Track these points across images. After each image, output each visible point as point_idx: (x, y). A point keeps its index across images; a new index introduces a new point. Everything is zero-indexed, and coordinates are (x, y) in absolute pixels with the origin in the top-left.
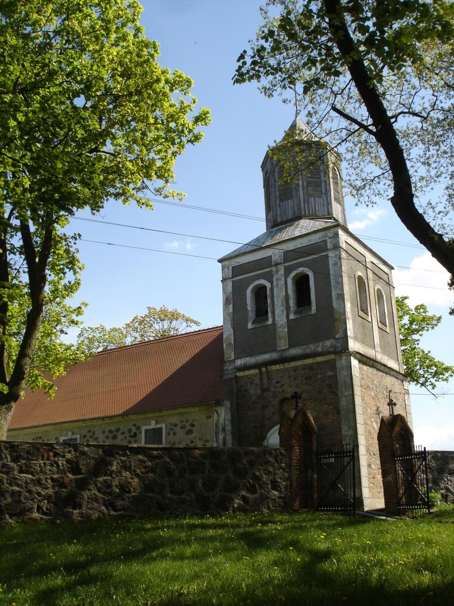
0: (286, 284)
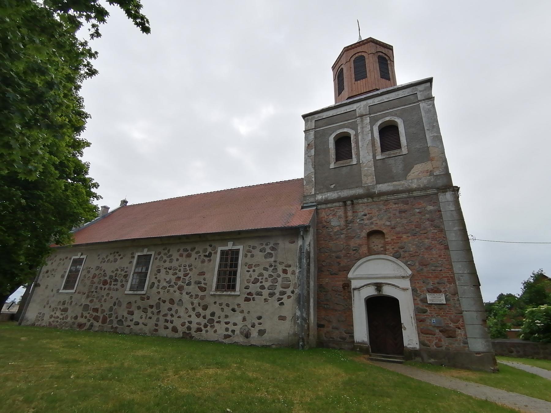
0: (372, 130)
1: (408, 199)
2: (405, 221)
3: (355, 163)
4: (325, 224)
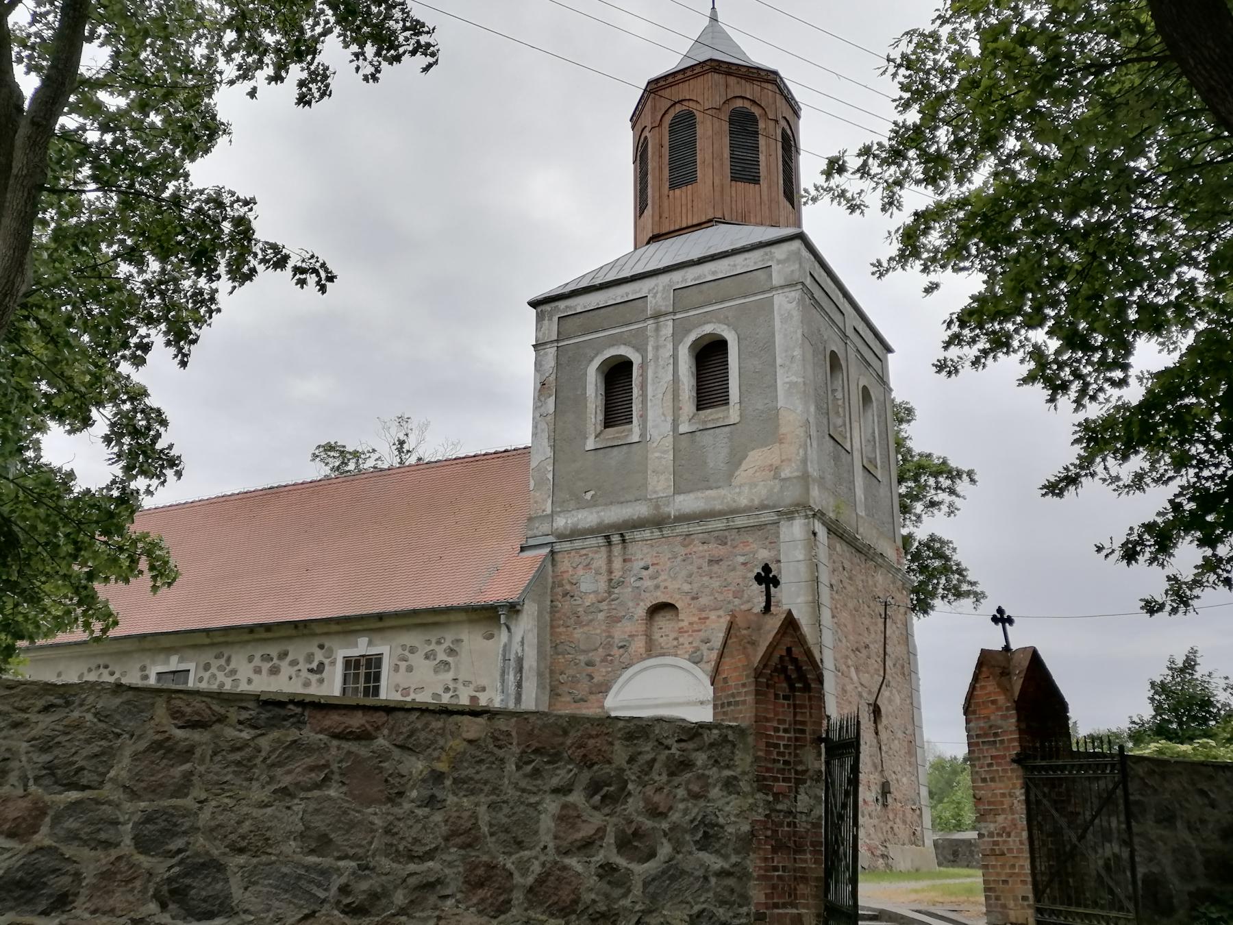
0: (675, 357)
1: (726, 533)
2: (716, 584)
3: (635, 438)
4: (568, 587)
